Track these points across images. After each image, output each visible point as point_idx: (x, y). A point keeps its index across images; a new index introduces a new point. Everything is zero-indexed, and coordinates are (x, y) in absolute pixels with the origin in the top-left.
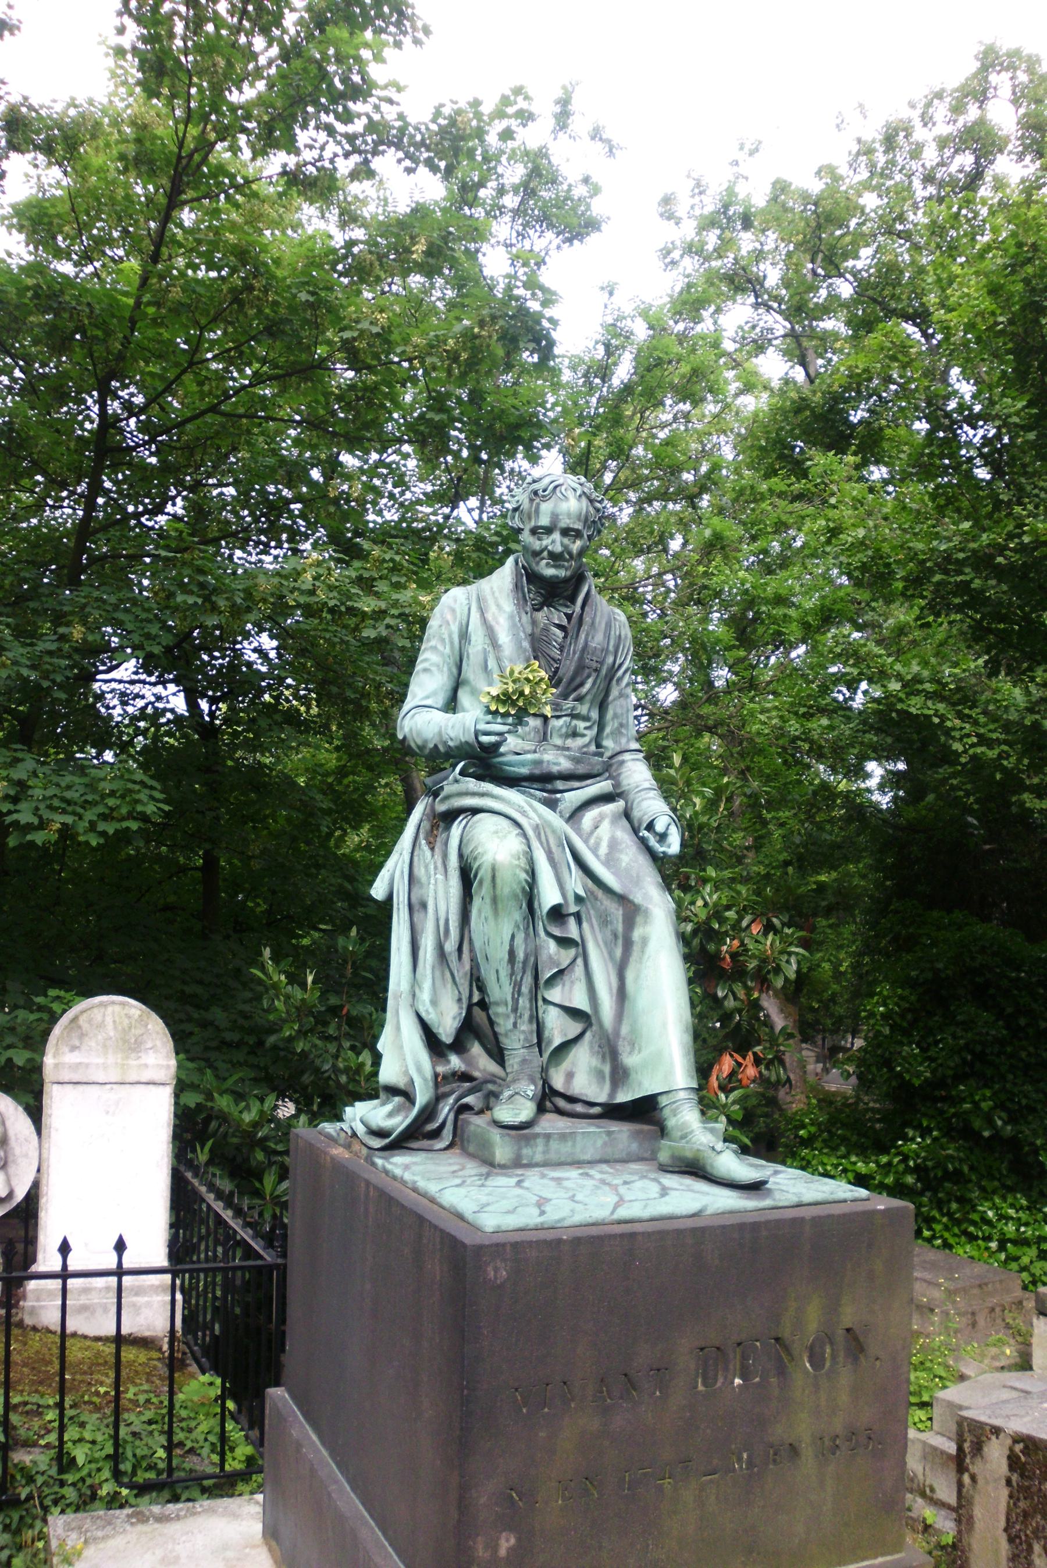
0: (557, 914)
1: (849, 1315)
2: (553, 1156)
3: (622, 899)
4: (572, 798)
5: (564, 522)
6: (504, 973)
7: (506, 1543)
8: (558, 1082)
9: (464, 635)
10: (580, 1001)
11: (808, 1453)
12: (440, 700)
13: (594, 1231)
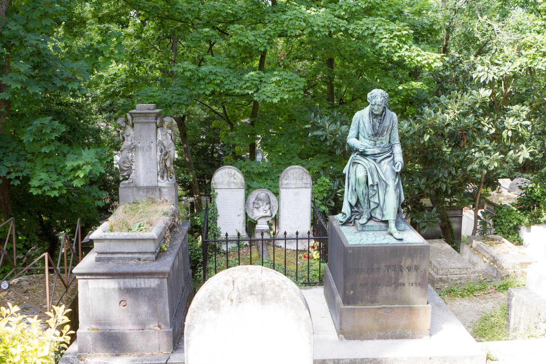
0: (373, 186)
1: (415, 263)
3: (385, 182)
4: (379, 159)
5: (377, 103)
6: (362, 196)
7: (352, 292)
8: (373, 215)
9: (359, 123)
10: (377, 201)
11: (407, 285)
12: (355, 136)
13: (367, 246)
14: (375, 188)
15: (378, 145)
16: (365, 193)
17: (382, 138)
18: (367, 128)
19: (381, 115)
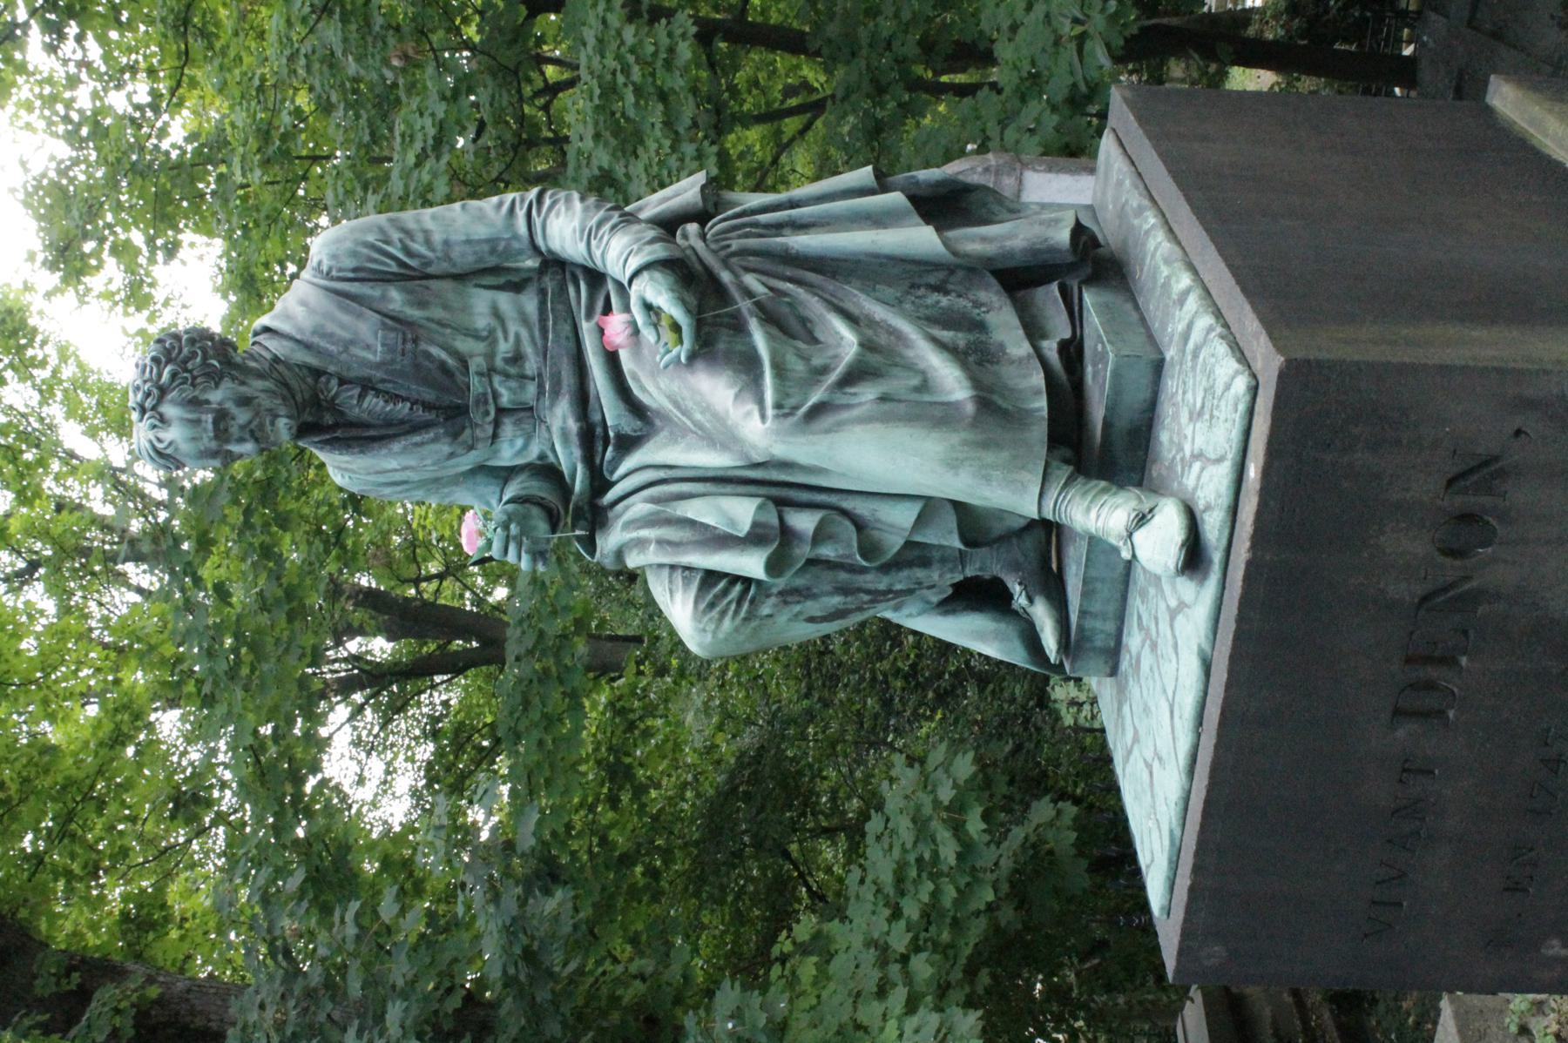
2: (1112, 608)
5: (208, 442)
14: (804, 522)
15: (532, 389)
16: (836, 601)
17: (476, 363)
18: (413, 463)
19: (317, 373)
